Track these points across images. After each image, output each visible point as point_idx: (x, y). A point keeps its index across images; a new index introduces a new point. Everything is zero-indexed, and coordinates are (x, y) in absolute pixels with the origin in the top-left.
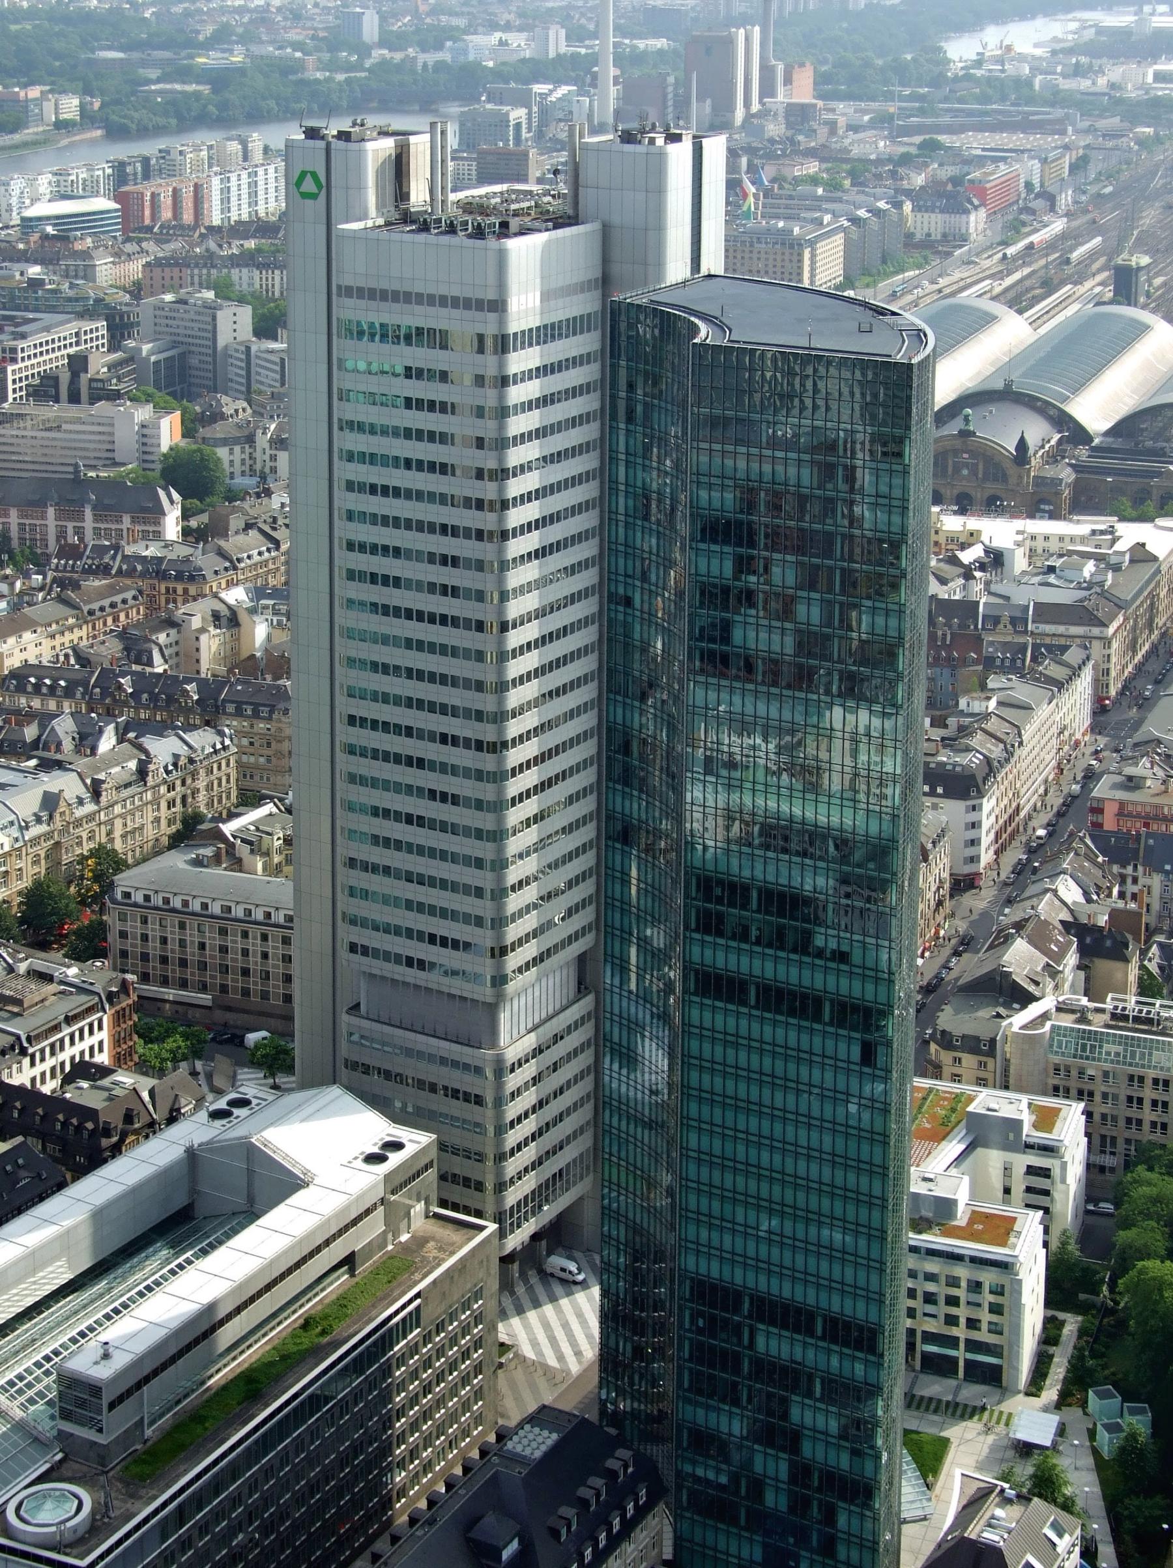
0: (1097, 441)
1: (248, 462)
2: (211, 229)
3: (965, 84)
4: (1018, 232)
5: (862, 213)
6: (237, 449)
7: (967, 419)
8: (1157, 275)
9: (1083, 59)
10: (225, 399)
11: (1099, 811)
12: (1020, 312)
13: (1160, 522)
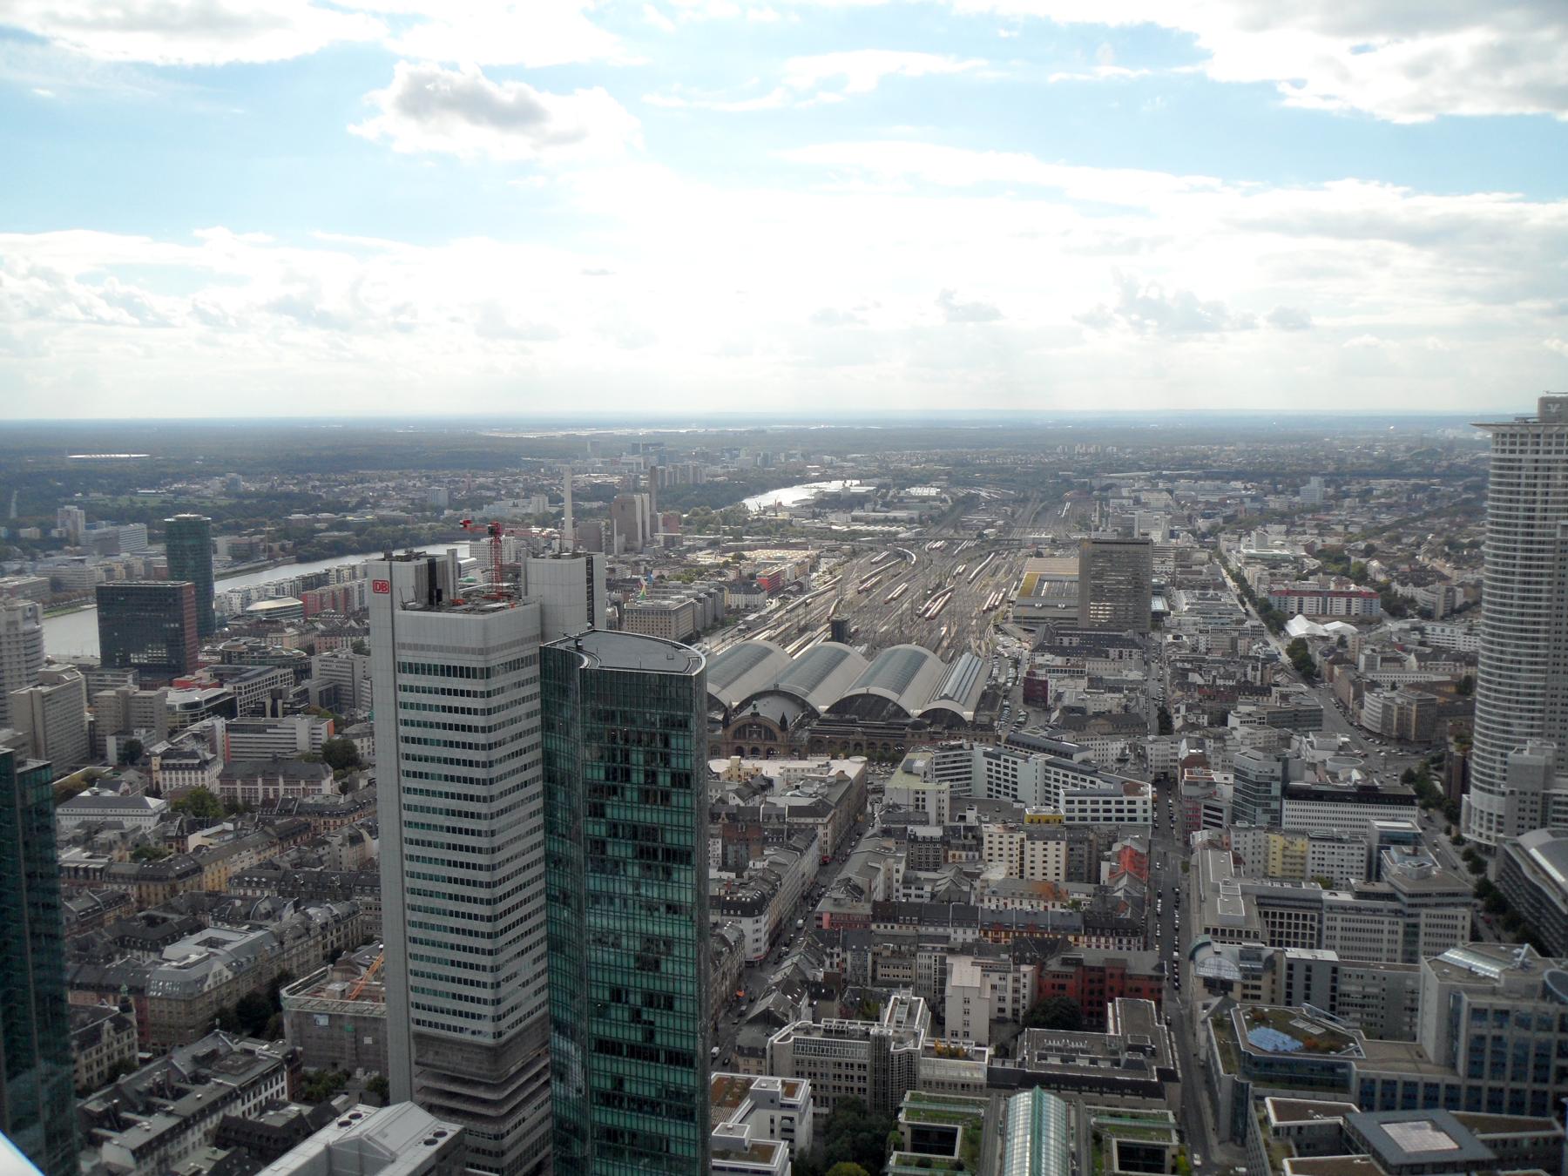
0: (823, 715)
2: (354, 613)
7: (755, 707)
9: (817, 510)
10: (359, 712)
11: (820, 919)
13: (852, 759)
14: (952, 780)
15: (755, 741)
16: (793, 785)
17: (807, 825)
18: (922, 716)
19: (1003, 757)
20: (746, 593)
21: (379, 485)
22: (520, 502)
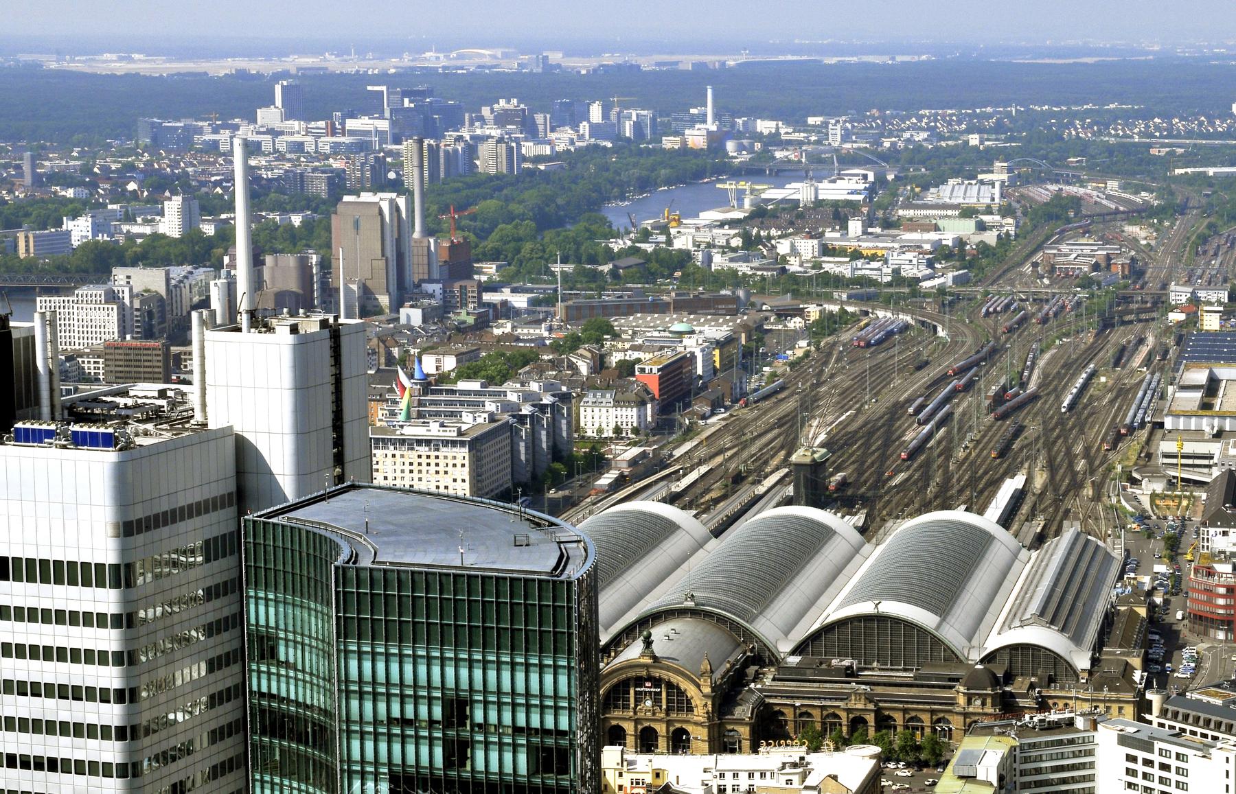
3: (633, 260)
19: (1158, 745)
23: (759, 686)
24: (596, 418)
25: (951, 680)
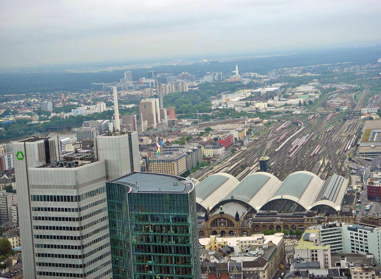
0: (258, 212)
1: (18, 242)
2: (5, 171)
3: (217, 111)
4: (234, 153)
5: (190, 151)
6: (15, 238)
7: (221, 209)
8: (272, 162)
12: (235, 176)
14: (331, 244)
15: (222, 227)
16: (245, 252)
17: (253, 271)
18: (312, 209)
19: (359, 230)
20: (213, 148)
21: (16, 102)
22: (92, 107)
23: (252, 219)
24: (208, 152)
25: (303, 215)
